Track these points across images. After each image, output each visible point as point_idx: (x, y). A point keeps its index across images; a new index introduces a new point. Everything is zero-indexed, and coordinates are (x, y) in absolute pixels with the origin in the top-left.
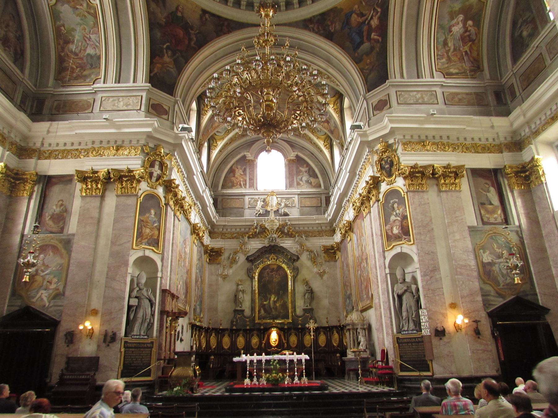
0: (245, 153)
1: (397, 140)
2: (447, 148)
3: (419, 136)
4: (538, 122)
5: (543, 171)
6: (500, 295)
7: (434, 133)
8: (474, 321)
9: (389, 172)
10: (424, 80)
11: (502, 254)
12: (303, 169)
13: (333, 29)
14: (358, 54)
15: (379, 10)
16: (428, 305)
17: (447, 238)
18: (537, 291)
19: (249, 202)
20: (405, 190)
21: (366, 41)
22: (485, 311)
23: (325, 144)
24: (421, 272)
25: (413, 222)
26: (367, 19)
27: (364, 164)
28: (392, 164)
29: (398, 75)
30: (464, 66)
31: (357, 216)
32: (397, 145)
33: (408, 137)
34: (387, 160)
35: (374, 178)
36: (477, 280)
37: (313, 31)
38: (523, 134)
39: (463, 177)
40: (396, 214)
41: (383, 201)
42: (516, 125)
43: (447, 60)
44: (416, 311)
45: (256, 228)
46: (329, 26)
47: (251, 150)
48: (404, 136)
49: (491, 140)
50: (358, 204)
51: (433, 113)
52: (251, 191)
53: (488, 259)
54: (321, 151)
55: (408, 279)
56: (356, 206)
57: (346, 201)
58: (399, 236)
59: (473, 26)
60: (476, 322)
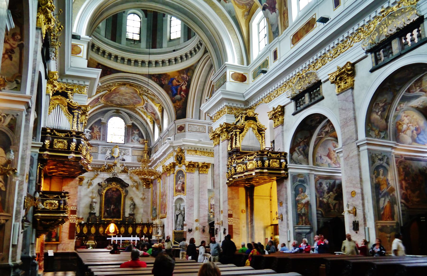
0: (101, 118)
3: (195, 148)
7: (201, 147)
12: (136, 132)
15: (186, 83)
17: (199, 193)
19: (102, 149)
26: (180, 84)
28: (182, 159)
29: (190, 117)
33: (190, 148)
37: (154, 81)
45: (106, 166)
46: (162, 81)
47: (104, 117)
52: (104, 143)
55: (182, 209)
60: (204, 227)
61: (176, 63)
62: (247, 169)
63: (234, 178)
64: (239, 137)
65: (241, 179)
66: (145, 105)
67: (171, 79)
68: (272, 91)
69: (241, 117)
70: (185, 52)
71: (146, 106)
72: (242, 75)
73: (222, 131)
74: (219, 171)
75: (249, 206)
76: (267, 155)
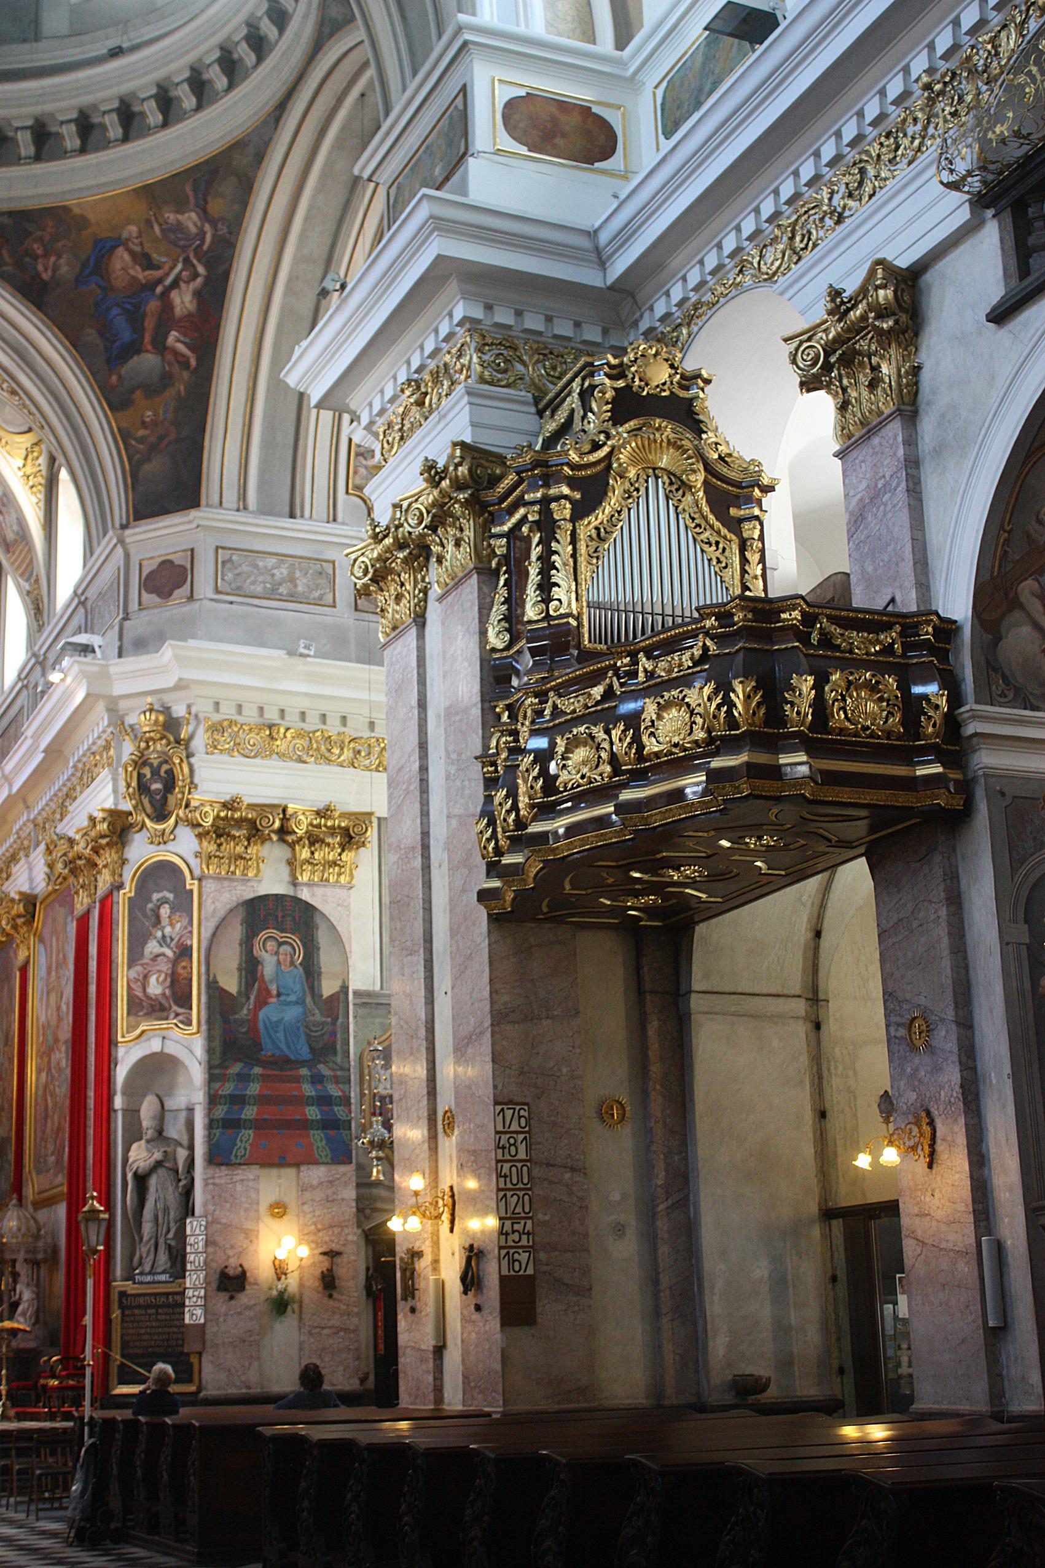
2: (336, 751)
3: (261, 709)
7: (304, 704)
8: (324, 1254)
9: (158, 805)
13: (50, 273)
14: (120, 377)
15: (201, 269)
16: (211, 1208)
21: (149, 347)
22: (358, 1227)
26: (160, 281)
28: (170, 783)
29: (231, 496)
32: (193, 723)
33: (228, 711)
40: (164, 936)
41: (130, 891)
44: (180, 1220)
46: (36, 258)
51: (306, 652)
55: (175, 1130)
58: (161, 1004)
61: (133, 133)
62: (640, 757)
63: (543, 837)
64: (574, 541)
65: (592, 840)
67: (97, 242)
68: (813, 182)
69: (586, 395)
70: (190, 58)
72: (586, 111)
73: (440, 517)
74: (425, 813)
75: (656, 1069)
76: (805, 638)
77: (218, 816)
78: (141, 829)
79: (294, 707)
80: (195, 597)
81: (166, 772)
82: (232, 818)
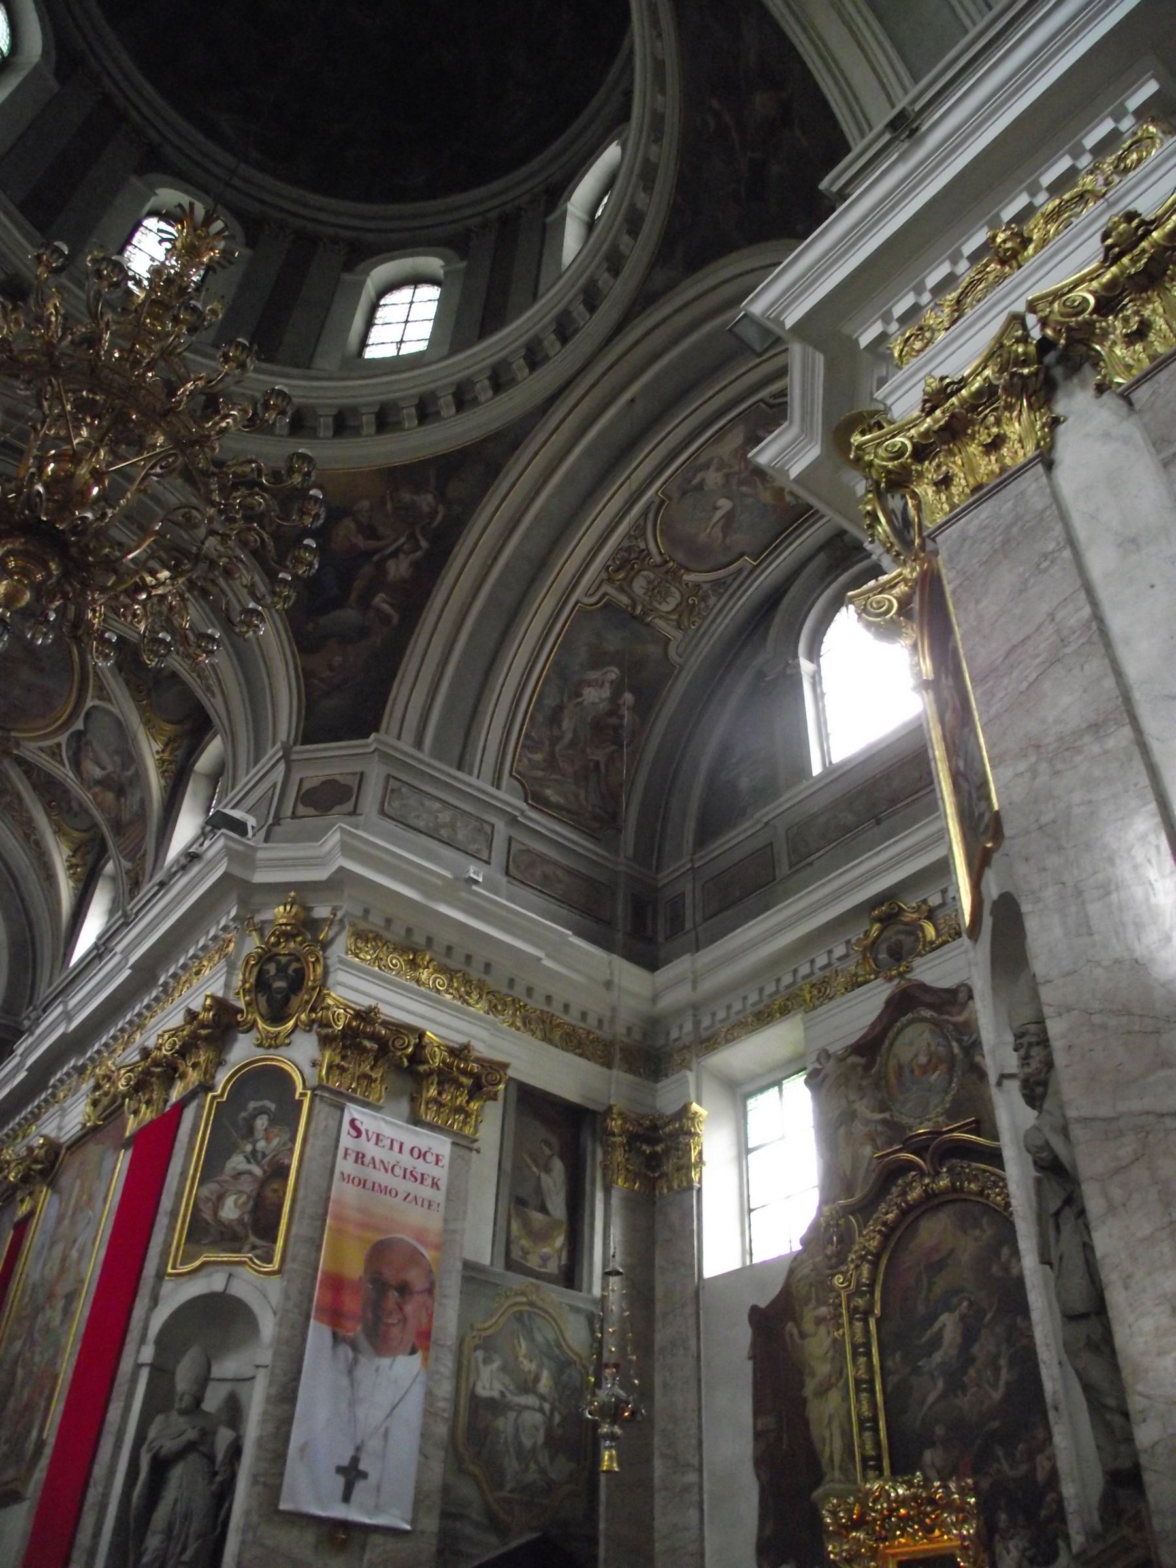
1: (340, 914)
2: (475, 996)
3: (409, 931)
4: (721, 1014)
5: (700, 1153)
6: (495, 1525)
7: (452, 938)
10: (473, 780)
11: (537, 1379)
18: (602, 1526)
20: (313, 1081)
23: (74, 861)
24: (271, 1384)
25: (301, 1194)
27: (200, 954)
28: (297, 982)
29: (409, 734)
30: (582, 797)
31: (95, 1129)
32: (335, 929)
33: (376, 920)
34: (289, 964)
35: (220, 1006)
36: (442, 1454)
38: (674, 1034)
39: (494, 1098)
40: (254, 1152)
41: (222, 1095)
42: (667, 1002)
43: (545, 760)
48: (367, 912)
49: (592, 1021)
50: (121, 1086)
53: (491, 1389)
54: (49, 877)
56: (106, 1094)
57: (74, 1067)
59: (634, 709)
66: (79, 725)
71: (79, 735)
77: (350, 1023)
78: (247, 1031)
79: (446, 937)
80: (358, 812)
81: (295, 971)
82: (364, 1032)
